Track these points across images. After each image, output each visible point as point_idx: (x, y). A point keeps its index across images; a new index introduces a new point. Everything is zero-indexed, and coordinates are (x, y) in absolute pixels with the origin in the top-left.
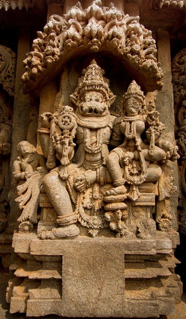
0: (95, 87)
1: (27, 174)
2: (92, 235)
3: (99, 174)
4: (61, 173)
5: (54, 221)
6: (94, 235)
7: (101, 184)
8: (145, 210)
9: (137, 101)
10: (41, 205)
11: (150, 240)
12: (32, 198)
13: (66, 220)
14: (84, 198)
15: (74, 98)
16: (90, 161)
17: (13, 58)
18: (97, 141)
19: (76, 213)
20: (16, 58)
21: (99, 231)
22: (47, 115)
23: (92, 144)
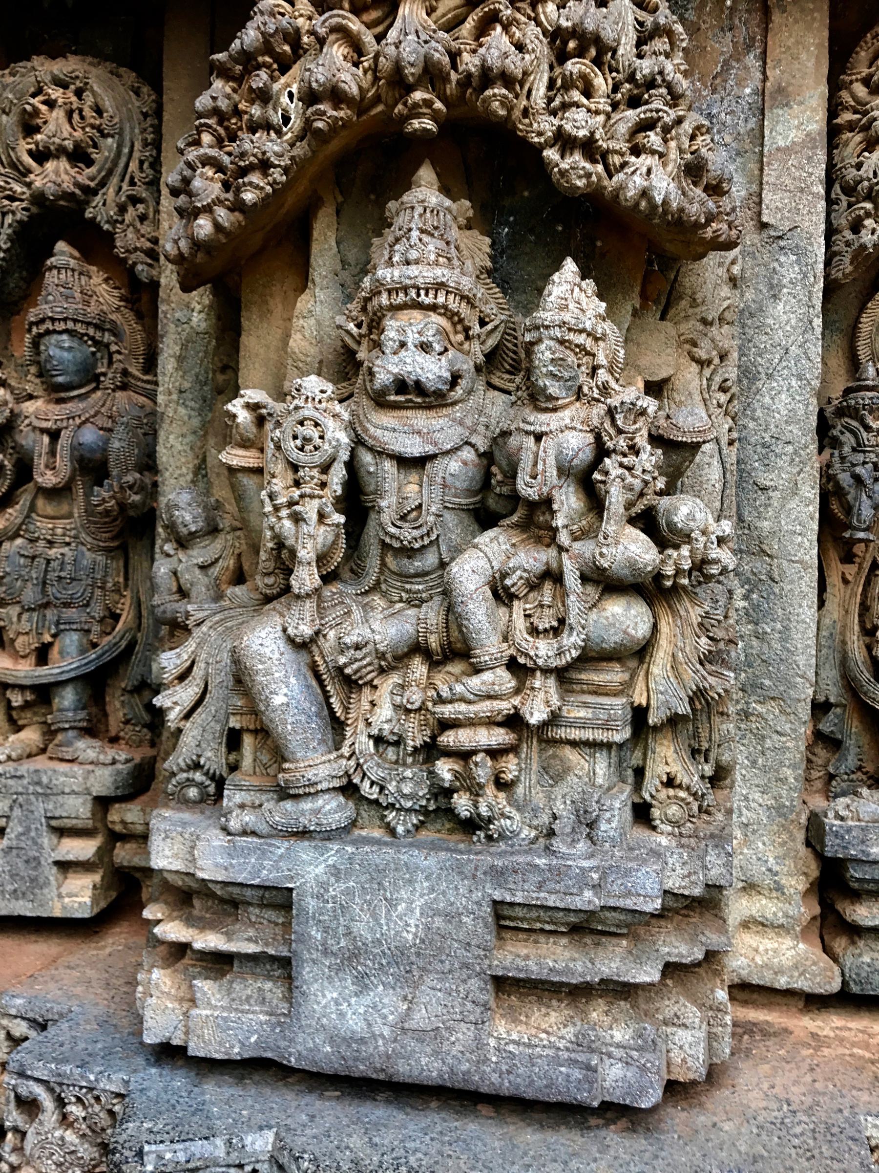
0: (419, 295)
6: (400, 829)
9: (568, 352)
14: (373, 704)
16: (400, 575)
17: (145, 115)
18: (420, 505)
20: (158, 112)
21: (421, 818)
22: (248, 406)
23: (406, 515)
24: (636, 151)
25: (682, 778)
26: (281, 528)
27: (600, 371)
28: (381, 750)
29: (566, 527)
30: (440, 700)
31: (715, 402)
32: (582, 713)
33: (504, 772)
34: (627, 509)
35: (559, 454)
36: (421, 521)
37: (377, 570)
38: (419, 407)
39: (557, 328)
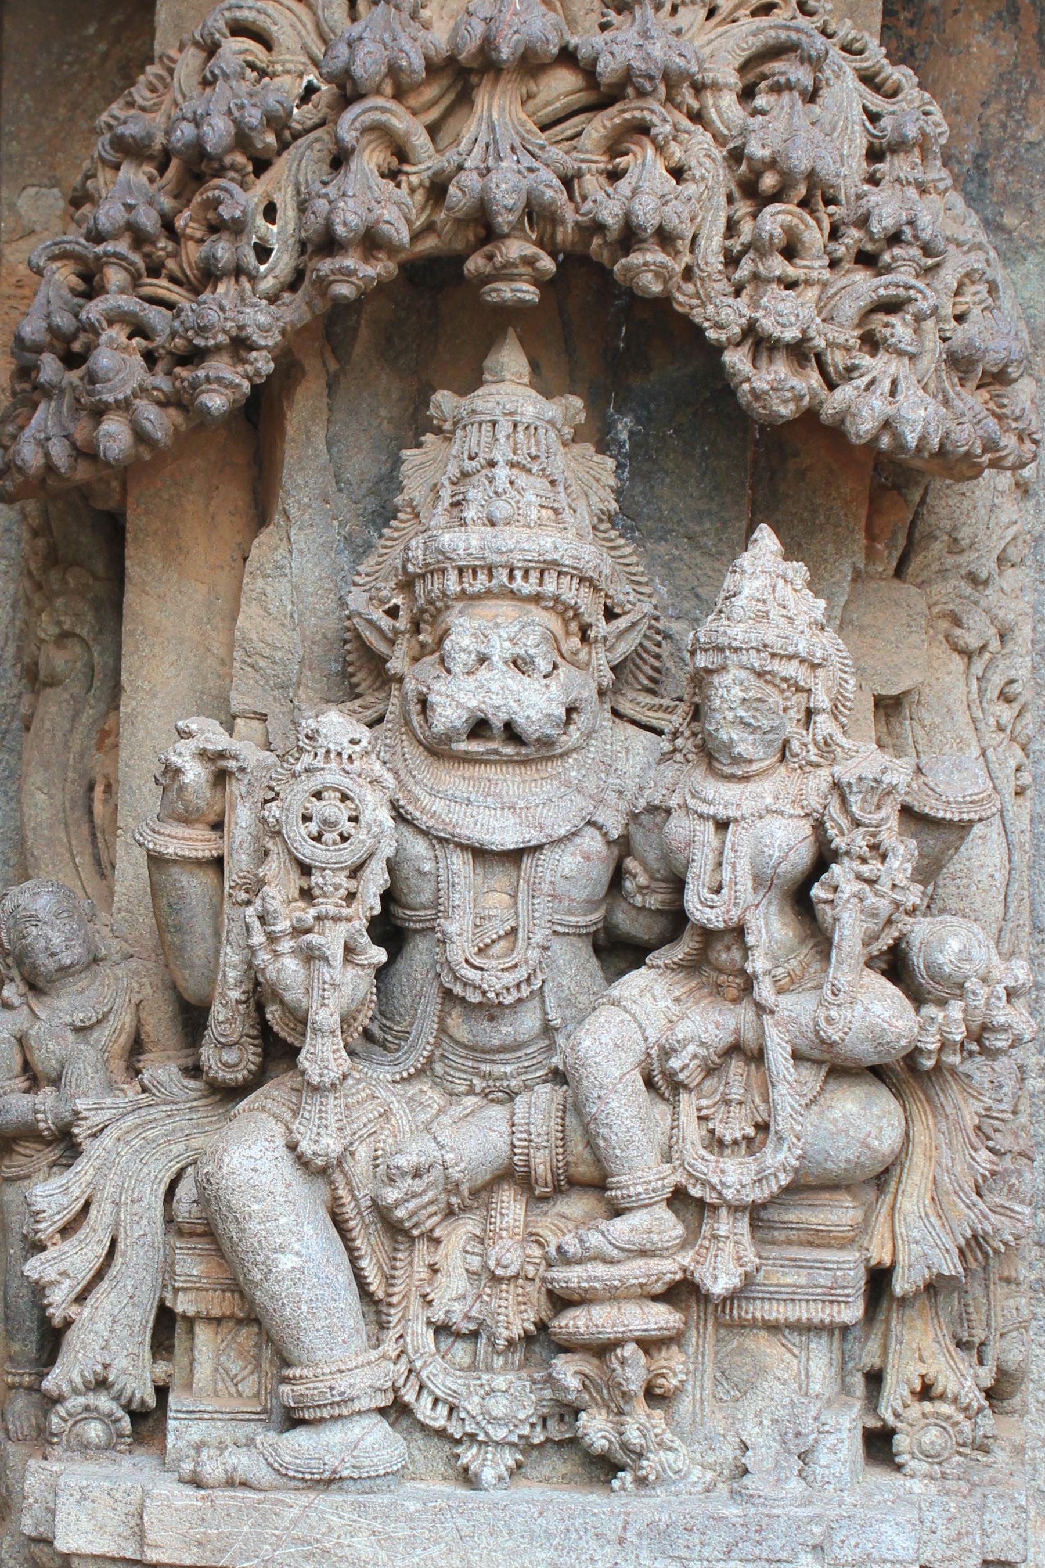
0: (511, 577)
1: (85, 1114)
2: (476, 1475)
3: (524, 1136)
4: (302, 1129)
5: (257, 1395)
6: (488, 1475)
7: (537, 1192)
8: (796, 1351)
9: (769, 689)
10: (183, 1305)
11: (793, 1511)
12: (118, 1260)
13: (331, 1388)
14: (433, 1269)
15: (370, 622)
16: (472, 1049)
18: (514, 930)
19: (384, 1357)
21: (520, 1457)
22: (203, 755)
23: (487, 946)
24: (871, 343)
25: (946, 1381)
26: (279, 971)
27: (819, 718)
28: (443, 1347)
29: (767, 973)
30: (565, 1259)
31: (992, 721)
32: (791, 1278)
33: (663, 1376)
34: (866, 944)
35: (757, 856)
36: (515, 958)
37: (432, 1040)
38: (510, 761)
39: (753, 652)
